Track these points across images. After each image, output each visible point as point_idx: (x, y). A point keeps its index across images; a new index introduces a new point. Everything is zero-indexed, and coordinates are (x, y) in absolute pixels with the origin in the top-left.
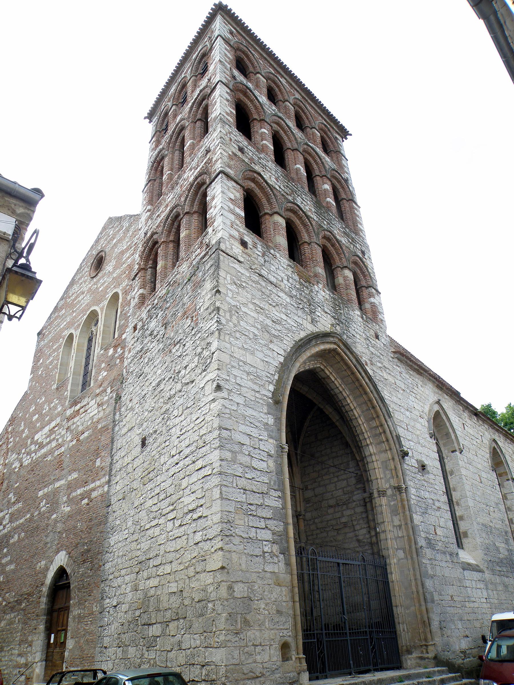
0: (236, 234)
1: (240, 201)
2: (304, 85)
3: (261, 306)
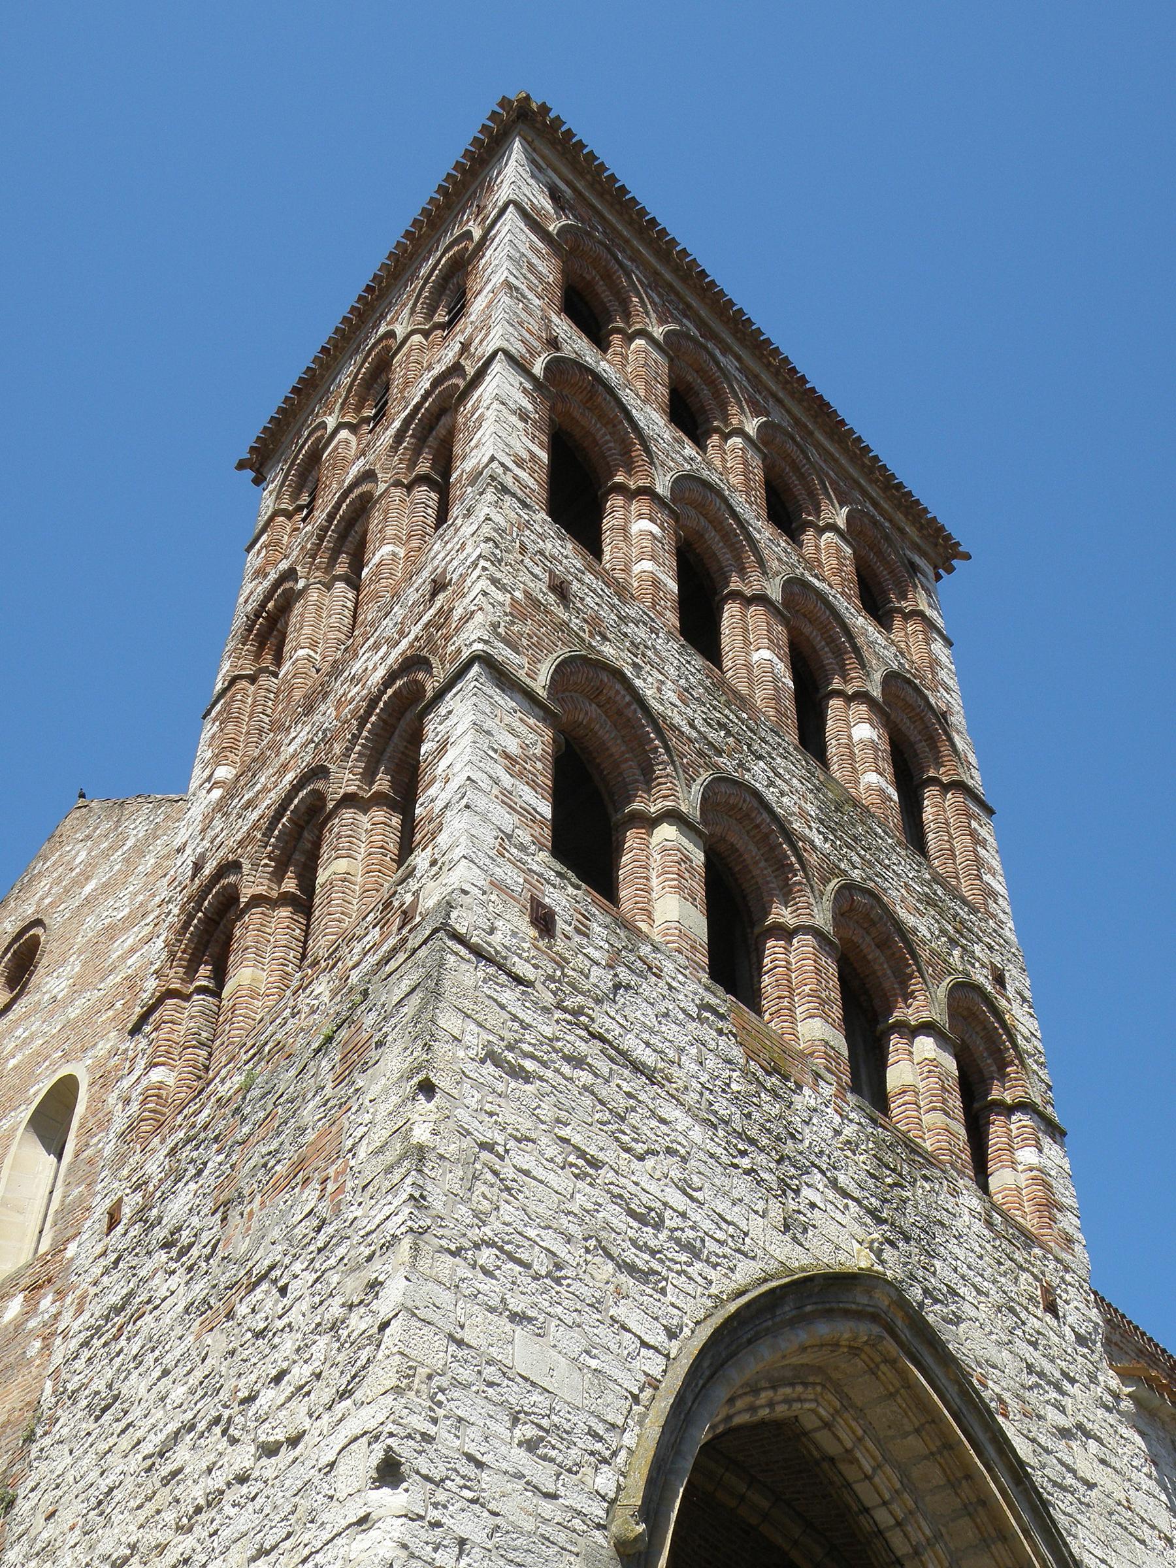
0: (512, 877)
1: (539, 765)
2: (803, 380)
3: (592, 1151)
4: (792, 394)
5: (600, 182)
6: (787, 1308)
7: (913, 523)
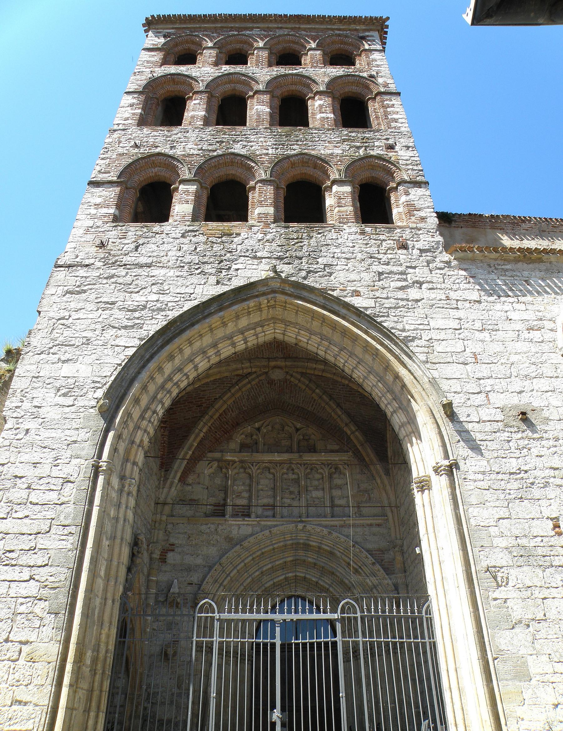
2: (286, 16)
4: (286, 22)
5: (182, 20)
7: (360, 24)
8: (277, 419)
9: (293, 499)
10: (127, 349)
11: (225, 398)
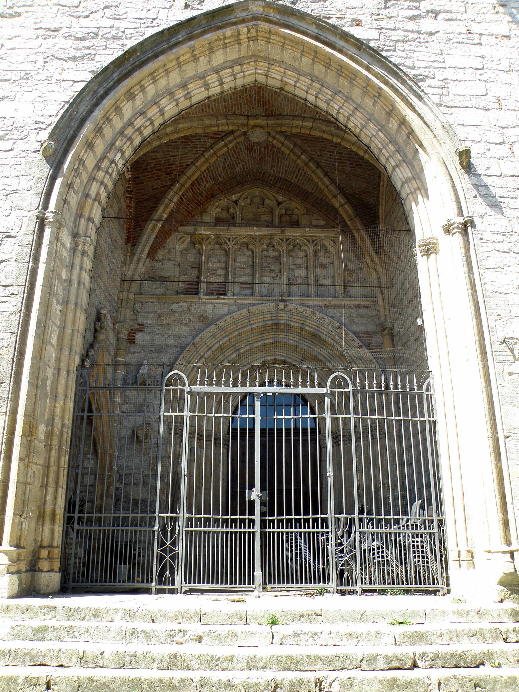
6: (179, 36)
8: (257, 192)
9: (273, 277)
10: (76, 84)
11: (197, 164)
